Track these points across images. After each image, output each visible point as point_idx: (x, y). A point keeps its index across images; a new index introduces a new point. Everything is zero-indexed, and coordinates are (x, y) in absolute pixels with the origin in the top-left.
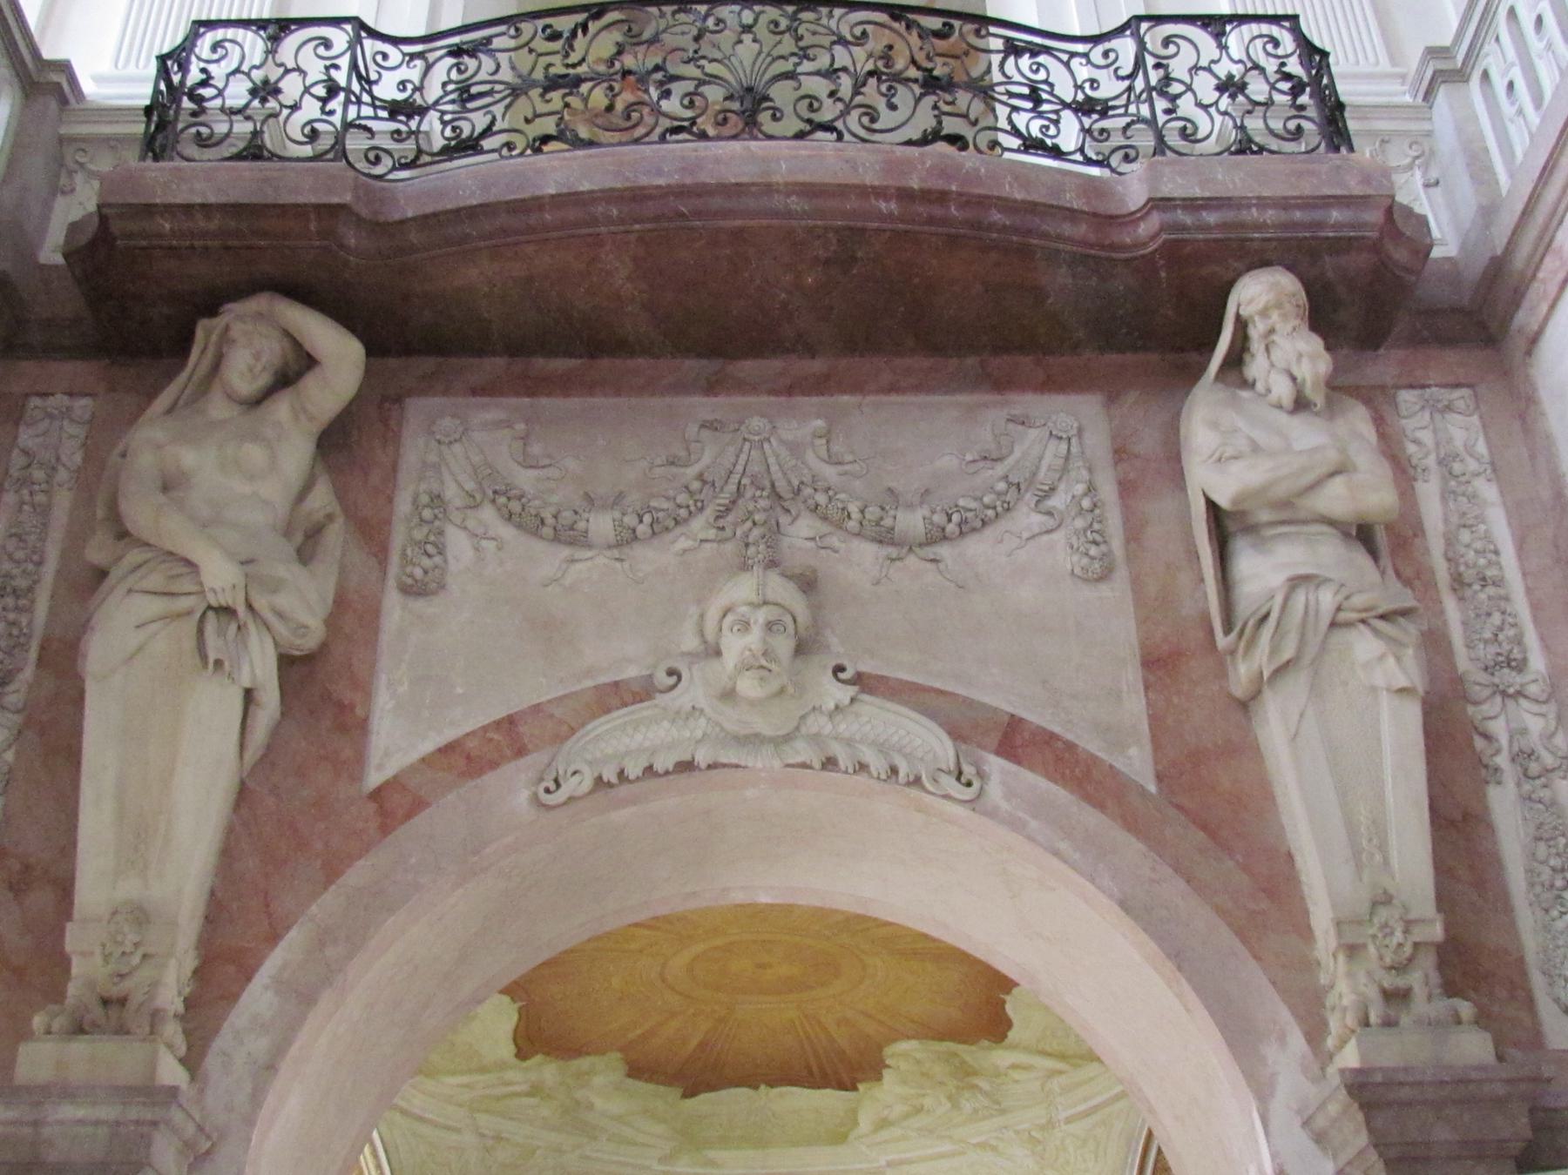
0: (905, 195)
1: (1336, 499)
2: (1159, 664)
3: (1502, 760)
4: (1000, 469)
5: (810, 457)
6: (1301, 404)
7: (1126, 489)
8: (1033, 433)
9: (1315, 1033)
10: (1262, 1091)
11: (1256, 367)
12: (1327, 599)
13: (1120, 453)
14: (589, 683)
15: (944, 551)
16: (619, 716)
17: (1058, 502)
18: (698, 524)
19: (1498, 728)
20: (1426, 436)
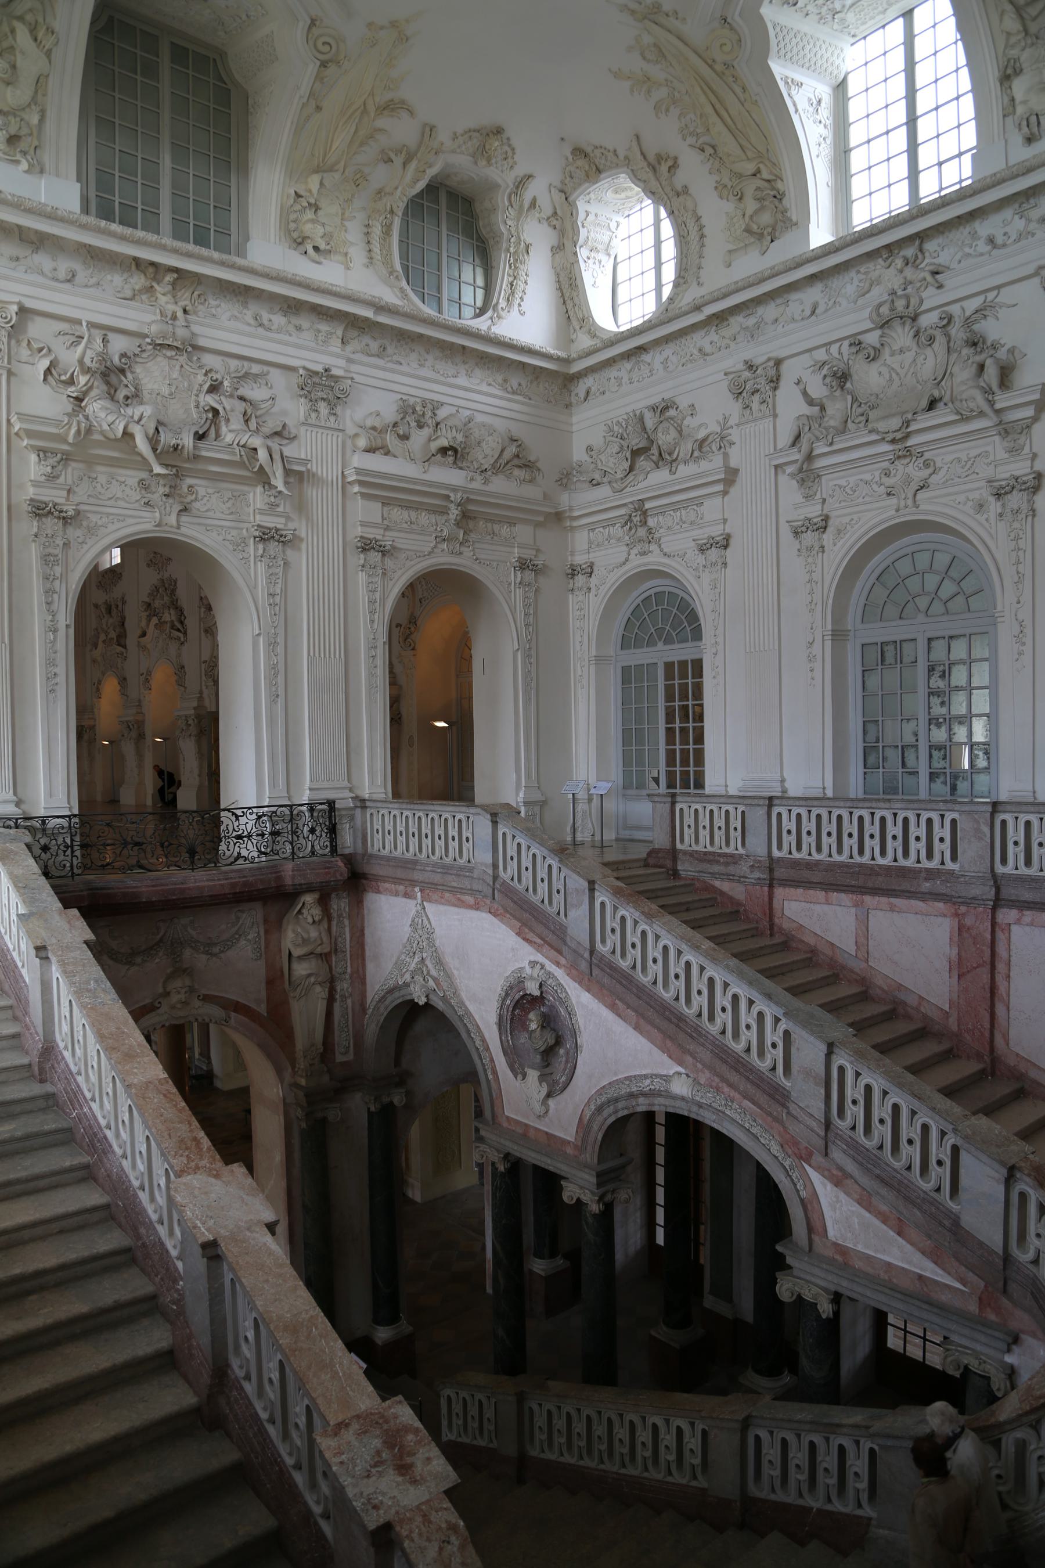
0: (235, 893)
1: (319, 950)
2: (270, 983)
3: (337, 997)
4: (236, 928)
5: (189, 929)
6: (314, 921)
7: (266, 932)
8: (244, 915)
9: (293, 1067)
10: (282, 1081)
11: (304, 911)
12: (313, 979)
13: (266, 921)
14: (137, 1006)
15: (222, 955)
16: (147, 1017)
17: (249, 937)
18: (161, 954)
19: (338, 988)
20: (335, 907)
